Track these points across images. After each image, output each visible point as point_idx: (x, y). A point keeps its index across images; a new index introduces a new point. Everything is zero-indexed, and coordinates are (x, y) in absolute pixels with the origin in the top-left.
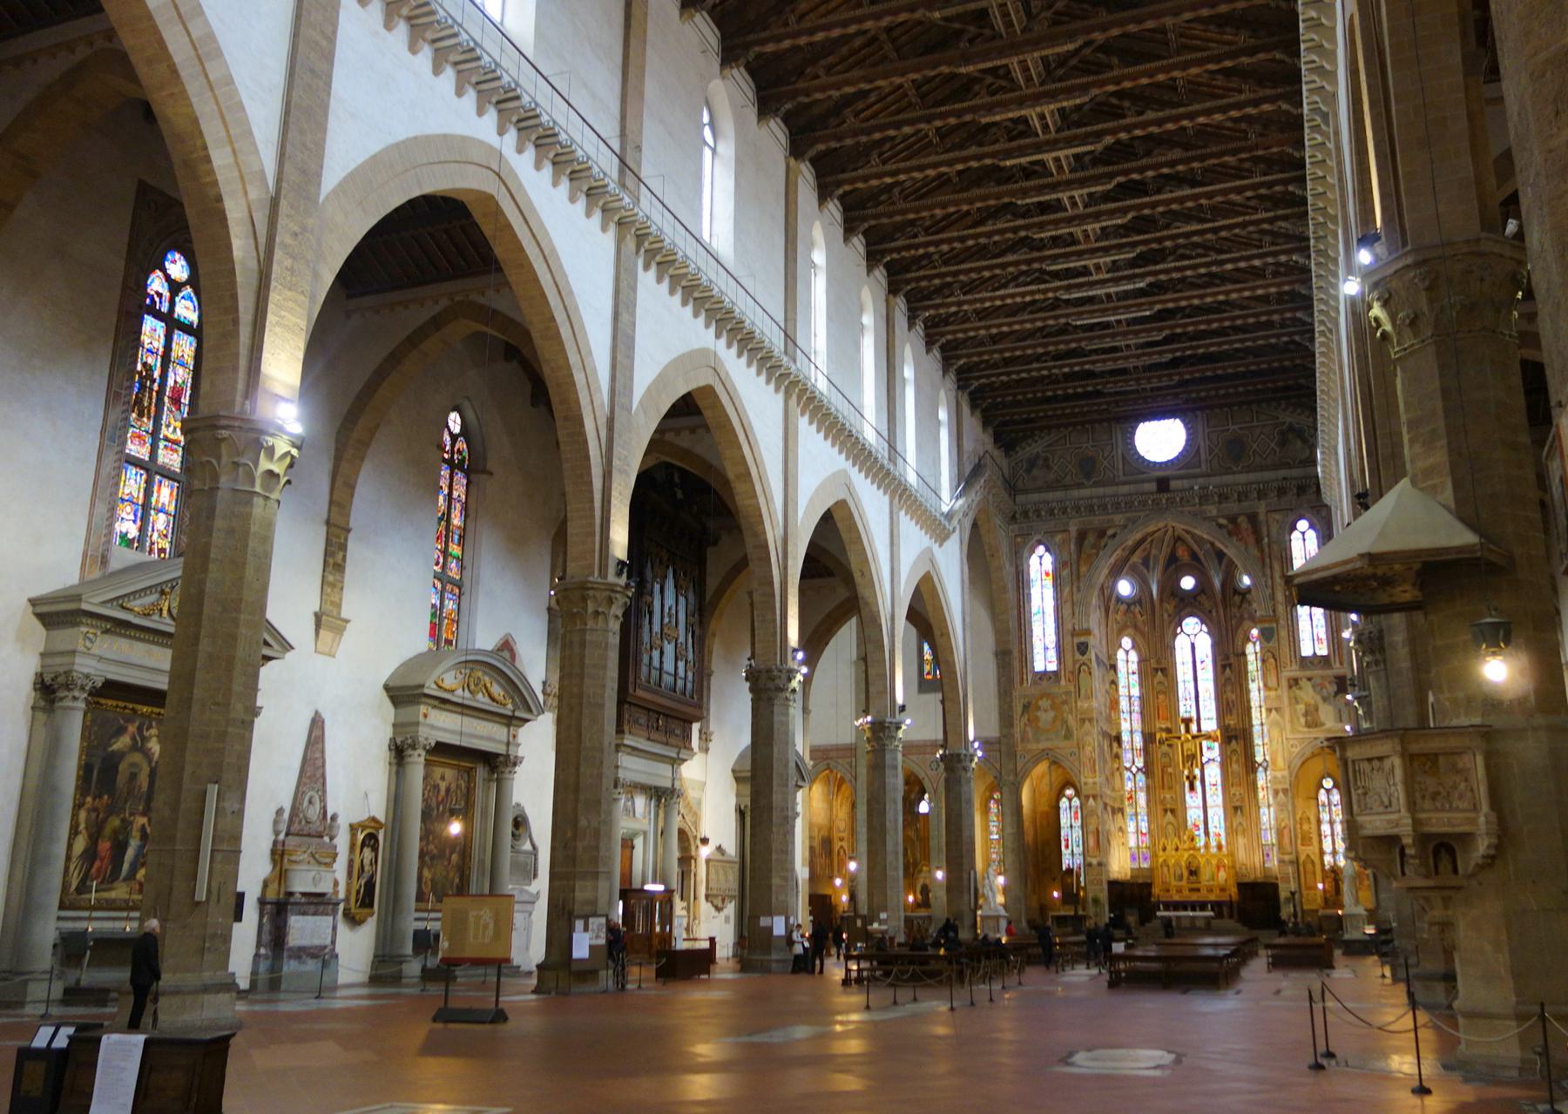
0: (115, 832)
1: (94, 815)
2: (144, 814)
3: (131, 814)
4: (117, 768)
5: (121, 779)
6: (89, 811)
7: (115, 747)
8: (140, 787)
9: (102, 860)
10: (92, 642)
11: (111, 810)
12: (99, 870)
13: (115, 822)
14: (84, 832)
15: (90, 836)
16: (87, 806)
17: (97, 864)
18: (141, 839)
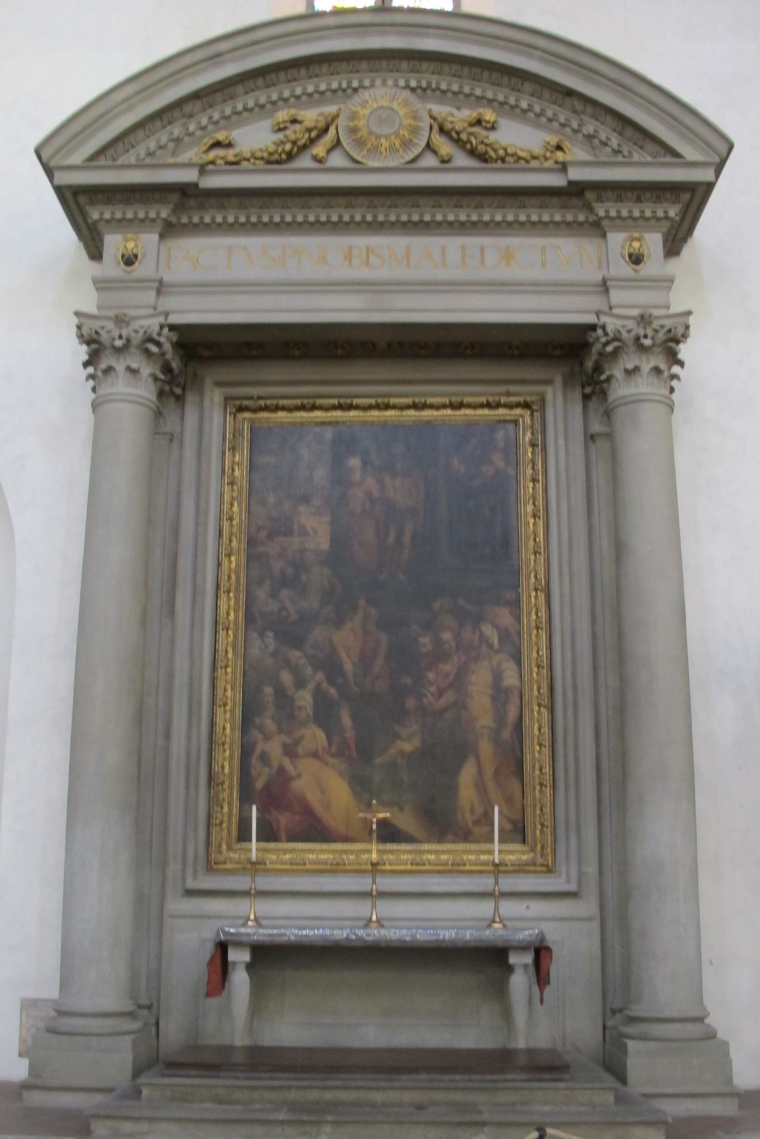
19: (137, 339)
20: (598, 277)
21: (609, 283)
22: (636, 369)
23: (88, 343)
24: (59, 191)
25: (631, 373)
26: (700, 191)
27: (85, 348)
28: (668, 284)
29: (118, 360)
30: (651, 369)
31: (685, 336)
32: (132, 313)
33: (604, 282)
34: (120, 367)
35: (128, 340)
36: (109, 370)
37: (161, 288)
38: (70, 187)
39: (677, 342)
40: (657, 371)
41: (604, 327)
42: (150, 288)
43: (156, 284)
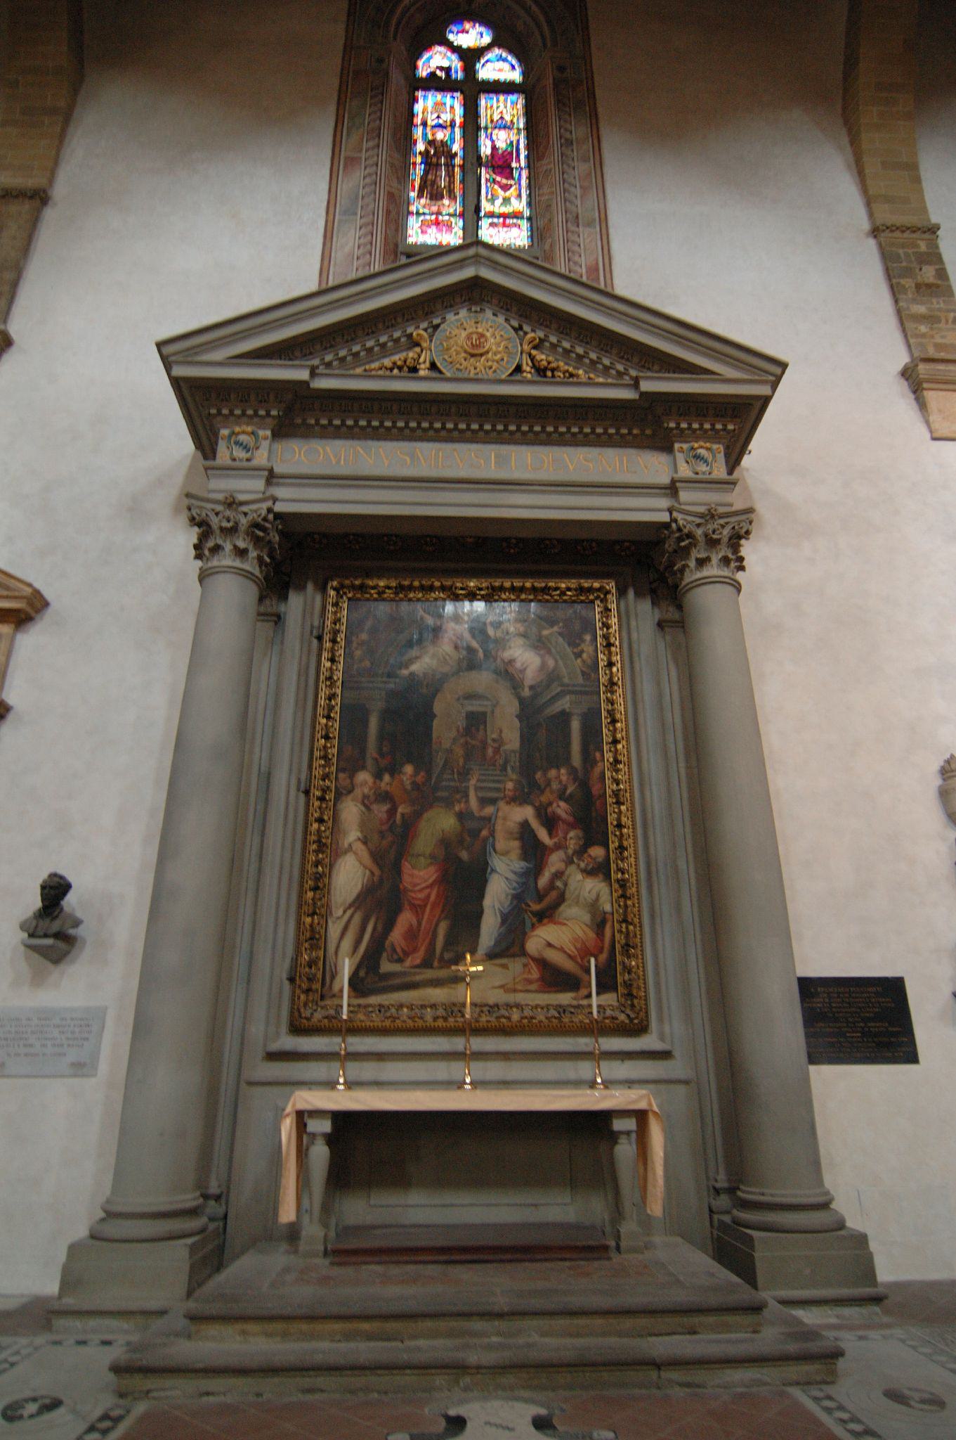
0: (446, 843)
1: (381, 810)
2: (520, 798)
3: (484, 802)
4: (428, 705)
5: (445, 731)
6: (366, 802)
7: (415, 667)
8: (499, 742)
9: (418, 909)
10: (246, 448)
11: (424, 798)
12: (411, 934)
13: (441, 822)
14: (359, 847)
15: (377, 857)
16: (358, 792)
17: (406, 919)
18: (525, 856)
19: (244, 521)
20: (666, 480)
21: (678, 485)
22: (708, 559)
23: (199, 525)
24: (176, 383)
25: (702, 563)
26: (758, 405)
27: (196, 529)
28: (732, 486)
29: (225, 541)
30: (720, 560)
31: (748, 532)
32: (241, 497)
33: (673, 482)
34: (228, 547)
35: (236, 523)
36: (216, 549)
37: (271, 477)
38: (187, 380)
39: (740, 537)
40: (726, 561)
41: (676, 521)
42: (261, 476)
43: (266, 473)
